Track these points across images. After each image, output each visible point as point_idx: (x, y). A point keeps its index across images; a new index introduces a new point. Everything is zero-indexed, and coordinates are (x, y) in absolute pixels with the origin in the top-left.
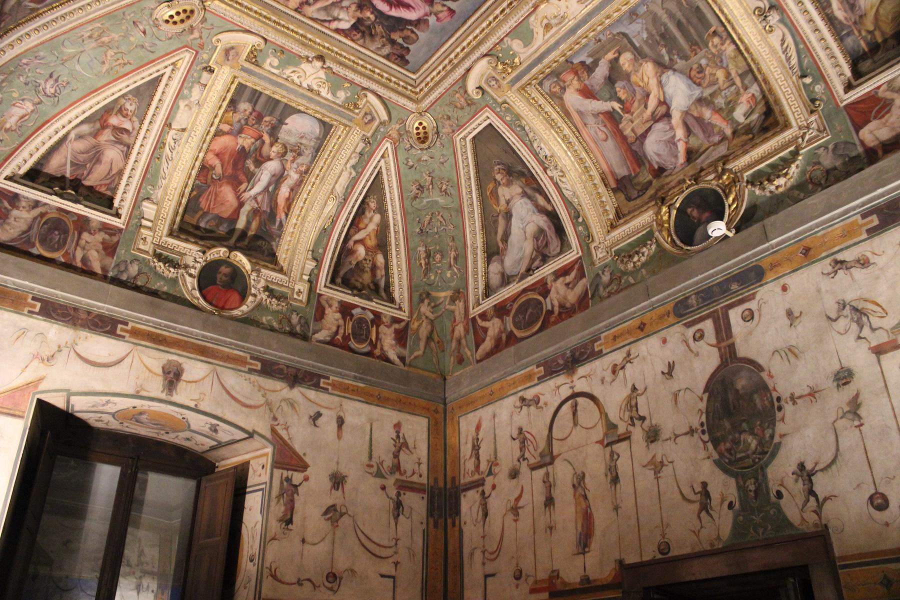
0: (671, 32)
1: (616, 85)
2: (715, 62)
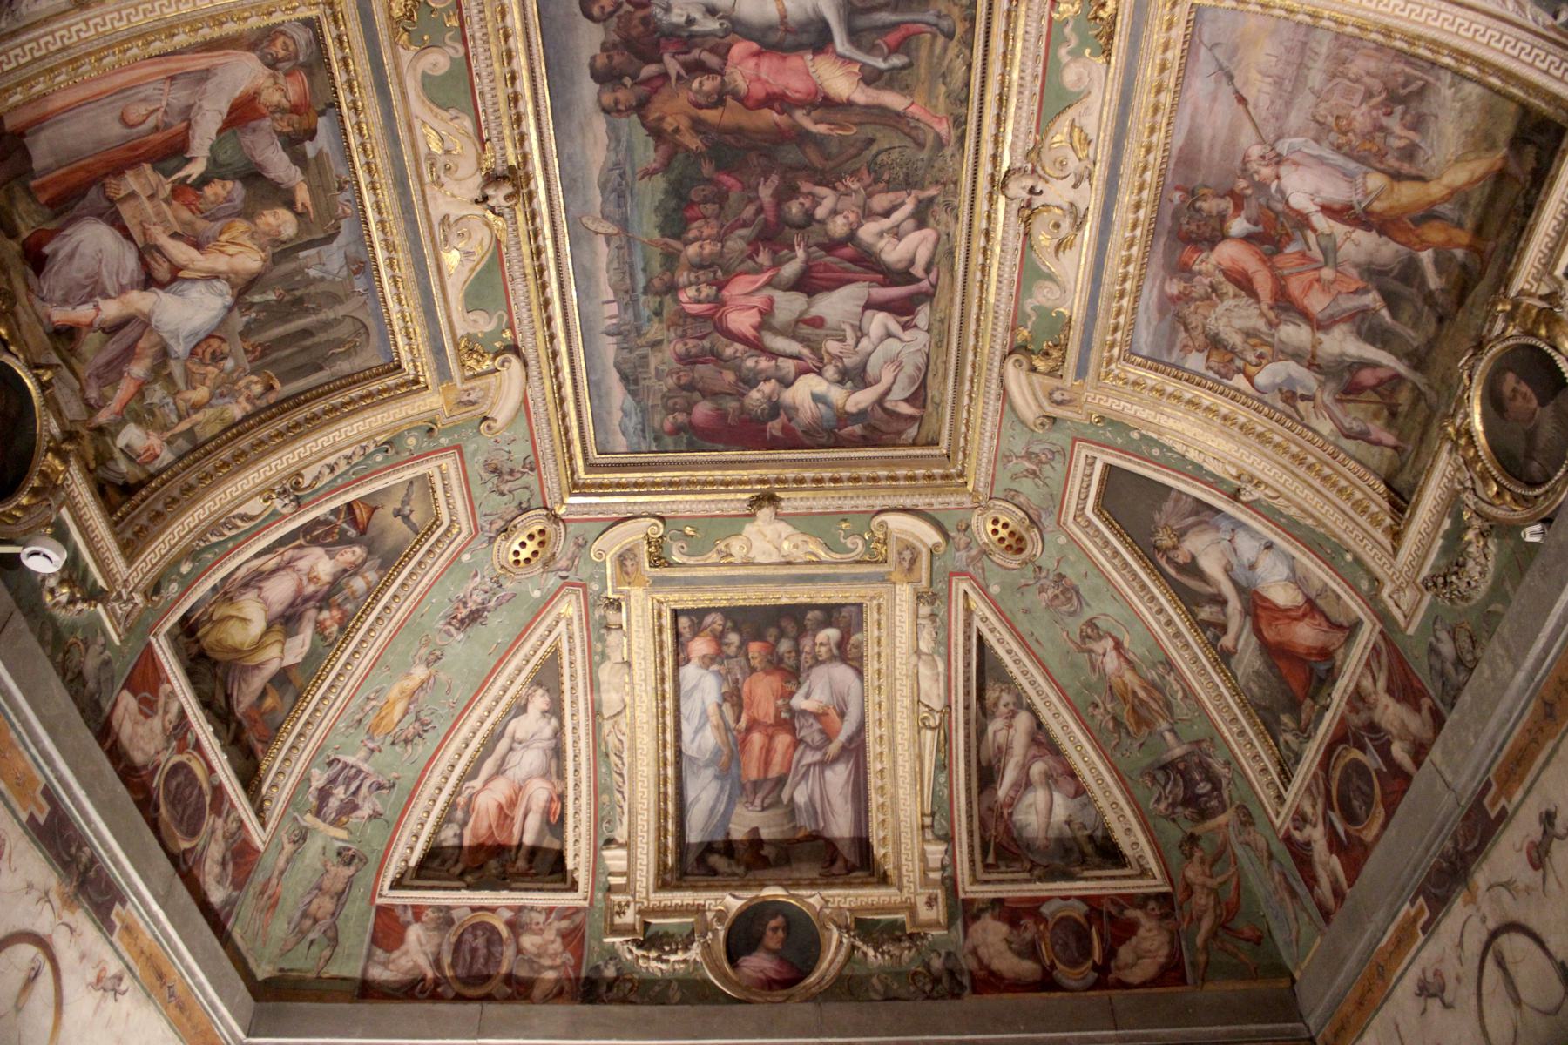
1: (239, 185)
2: (223, 384)
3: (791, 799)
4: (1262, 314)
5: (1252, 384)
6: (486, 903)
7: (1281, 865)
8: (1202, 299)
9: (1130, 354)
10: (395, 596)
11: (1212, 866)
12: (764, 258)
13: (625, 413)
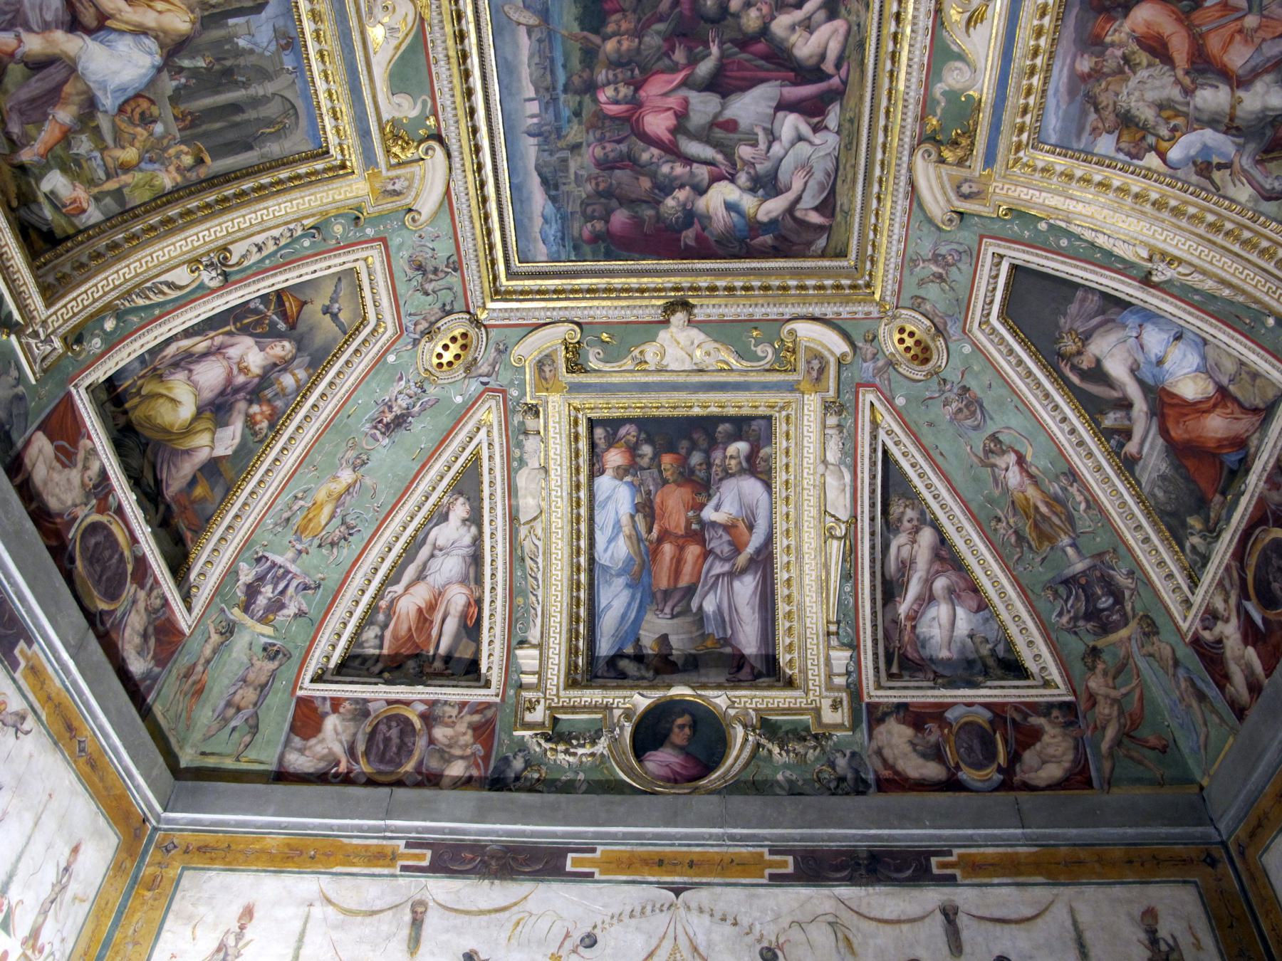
0: (229, 91)
3: (700, 608)
4: (1178, 82)
5: (1165, 161)
6: (401, 697)
7: (1188, 670)
8: (1114, 73)
9: (1038, 141)
10: (323, 395)
11: (1114, 678)
12: (679, 56)
13: (546, 220)
